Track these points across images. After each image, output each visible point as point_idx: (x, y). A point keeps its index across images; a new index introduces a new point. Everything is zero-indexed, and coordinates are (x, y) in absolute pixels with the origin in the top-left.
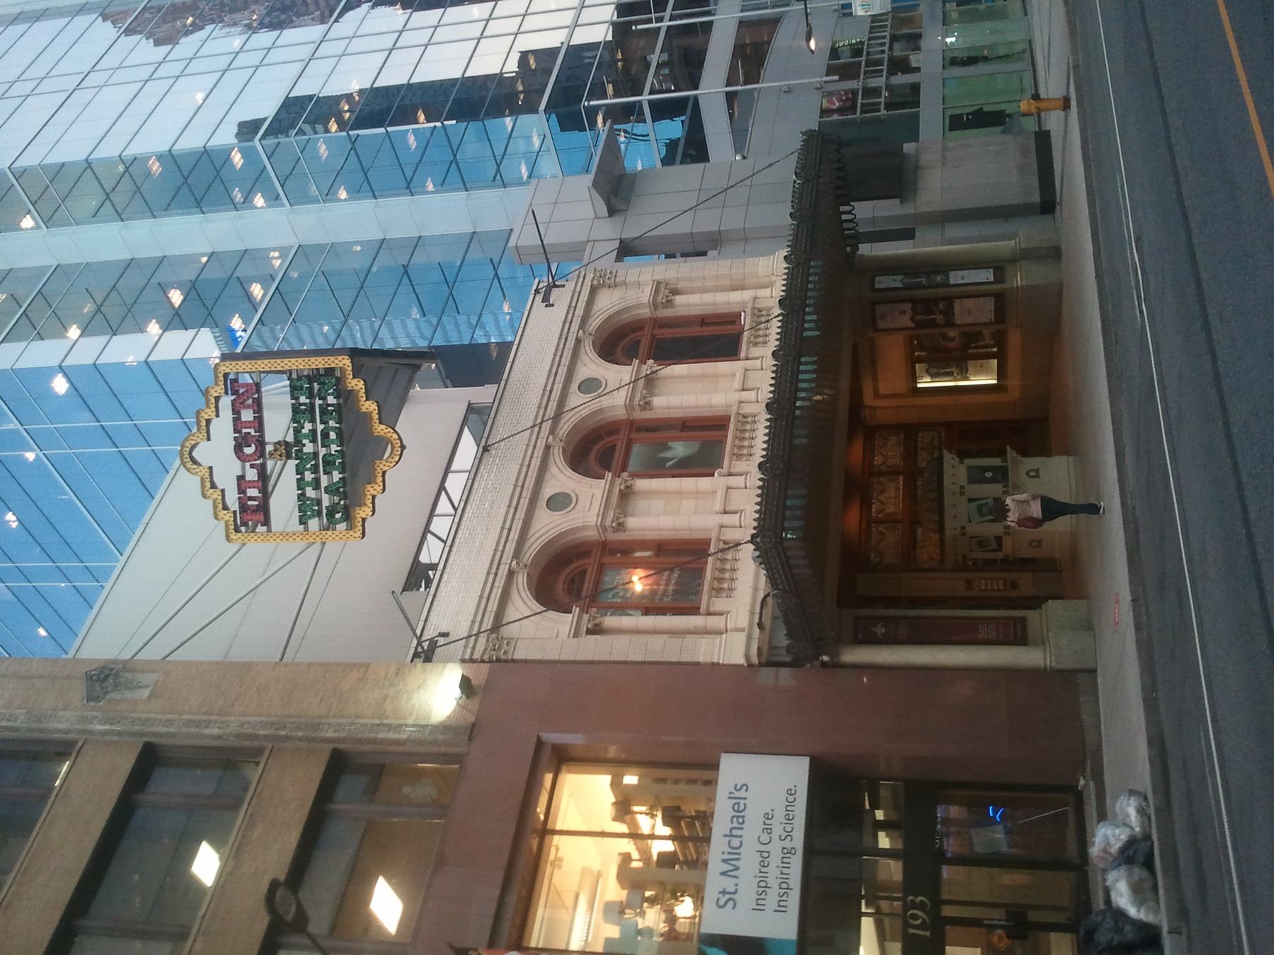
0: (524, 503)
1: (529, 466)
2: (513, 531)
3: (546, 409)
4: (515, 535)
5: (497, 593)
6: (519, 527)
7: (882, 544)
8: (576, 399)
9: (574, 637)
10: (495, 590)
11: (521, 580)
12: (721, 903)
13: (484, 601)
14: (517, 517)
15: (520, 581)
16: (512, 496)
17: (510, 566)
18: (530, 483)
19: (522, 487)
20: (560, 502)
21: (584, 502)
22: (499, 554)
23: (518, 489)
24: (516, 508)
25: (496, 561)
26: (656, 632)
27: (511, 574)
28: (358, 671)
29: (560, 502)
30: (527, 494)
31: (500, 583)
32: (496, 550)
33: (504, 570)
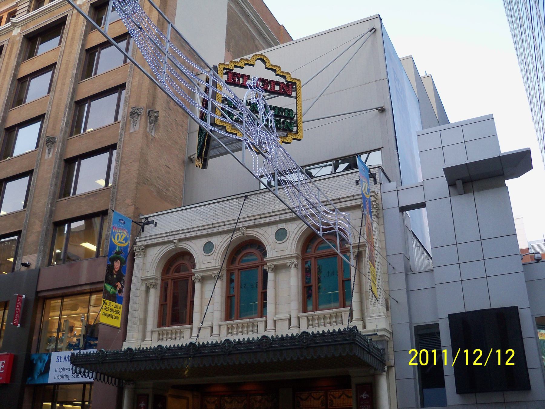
0: (205, 232)
1: (225, 225)
2: (190, 233)
3: (261, 218)
4: (188, 235)
5: (162, 240)
6: (204, 233)
7: (313, 399)
8: (272, 230)
9: (142, 279)
10: (163, 238)
11: (171, 246)
12: (58, 358)
13: (158, 236)
14: (197, 232)
15: (171, 246)
16: (207, 225)
17: (175, 240)
18: (216, 230)
19: (213, 227)
20: (208, 248)
21: (208, 259)
22: (179, 232)
23: (211, 226)
24: (201, 230)
25: (175, 233)
26: (146, 311)
27: (171, 242)
28: (131, 203)
29: (208, 248)
30: (210, 231)
31: (166, 239)
32: (180, 230)
33: (171, 238)
